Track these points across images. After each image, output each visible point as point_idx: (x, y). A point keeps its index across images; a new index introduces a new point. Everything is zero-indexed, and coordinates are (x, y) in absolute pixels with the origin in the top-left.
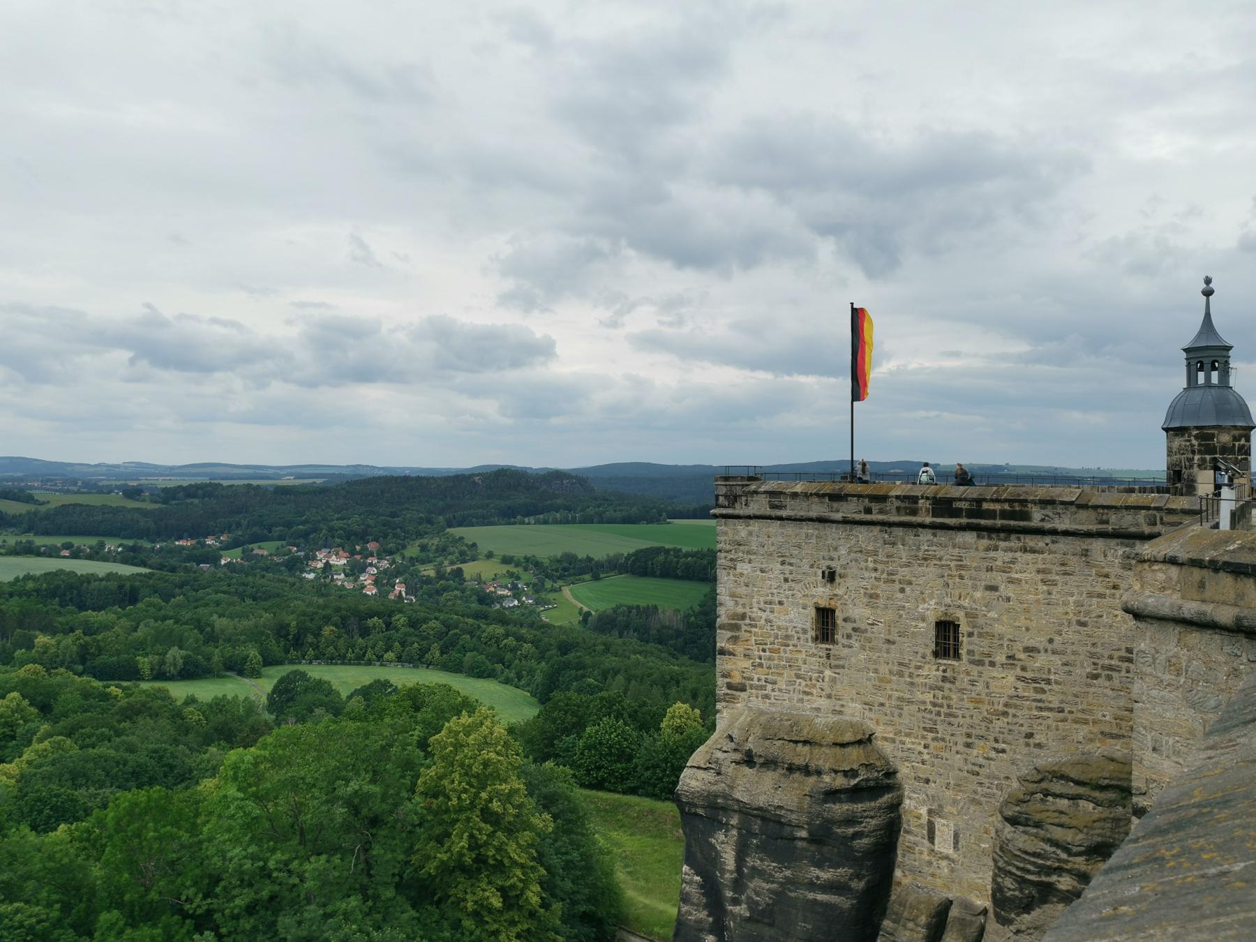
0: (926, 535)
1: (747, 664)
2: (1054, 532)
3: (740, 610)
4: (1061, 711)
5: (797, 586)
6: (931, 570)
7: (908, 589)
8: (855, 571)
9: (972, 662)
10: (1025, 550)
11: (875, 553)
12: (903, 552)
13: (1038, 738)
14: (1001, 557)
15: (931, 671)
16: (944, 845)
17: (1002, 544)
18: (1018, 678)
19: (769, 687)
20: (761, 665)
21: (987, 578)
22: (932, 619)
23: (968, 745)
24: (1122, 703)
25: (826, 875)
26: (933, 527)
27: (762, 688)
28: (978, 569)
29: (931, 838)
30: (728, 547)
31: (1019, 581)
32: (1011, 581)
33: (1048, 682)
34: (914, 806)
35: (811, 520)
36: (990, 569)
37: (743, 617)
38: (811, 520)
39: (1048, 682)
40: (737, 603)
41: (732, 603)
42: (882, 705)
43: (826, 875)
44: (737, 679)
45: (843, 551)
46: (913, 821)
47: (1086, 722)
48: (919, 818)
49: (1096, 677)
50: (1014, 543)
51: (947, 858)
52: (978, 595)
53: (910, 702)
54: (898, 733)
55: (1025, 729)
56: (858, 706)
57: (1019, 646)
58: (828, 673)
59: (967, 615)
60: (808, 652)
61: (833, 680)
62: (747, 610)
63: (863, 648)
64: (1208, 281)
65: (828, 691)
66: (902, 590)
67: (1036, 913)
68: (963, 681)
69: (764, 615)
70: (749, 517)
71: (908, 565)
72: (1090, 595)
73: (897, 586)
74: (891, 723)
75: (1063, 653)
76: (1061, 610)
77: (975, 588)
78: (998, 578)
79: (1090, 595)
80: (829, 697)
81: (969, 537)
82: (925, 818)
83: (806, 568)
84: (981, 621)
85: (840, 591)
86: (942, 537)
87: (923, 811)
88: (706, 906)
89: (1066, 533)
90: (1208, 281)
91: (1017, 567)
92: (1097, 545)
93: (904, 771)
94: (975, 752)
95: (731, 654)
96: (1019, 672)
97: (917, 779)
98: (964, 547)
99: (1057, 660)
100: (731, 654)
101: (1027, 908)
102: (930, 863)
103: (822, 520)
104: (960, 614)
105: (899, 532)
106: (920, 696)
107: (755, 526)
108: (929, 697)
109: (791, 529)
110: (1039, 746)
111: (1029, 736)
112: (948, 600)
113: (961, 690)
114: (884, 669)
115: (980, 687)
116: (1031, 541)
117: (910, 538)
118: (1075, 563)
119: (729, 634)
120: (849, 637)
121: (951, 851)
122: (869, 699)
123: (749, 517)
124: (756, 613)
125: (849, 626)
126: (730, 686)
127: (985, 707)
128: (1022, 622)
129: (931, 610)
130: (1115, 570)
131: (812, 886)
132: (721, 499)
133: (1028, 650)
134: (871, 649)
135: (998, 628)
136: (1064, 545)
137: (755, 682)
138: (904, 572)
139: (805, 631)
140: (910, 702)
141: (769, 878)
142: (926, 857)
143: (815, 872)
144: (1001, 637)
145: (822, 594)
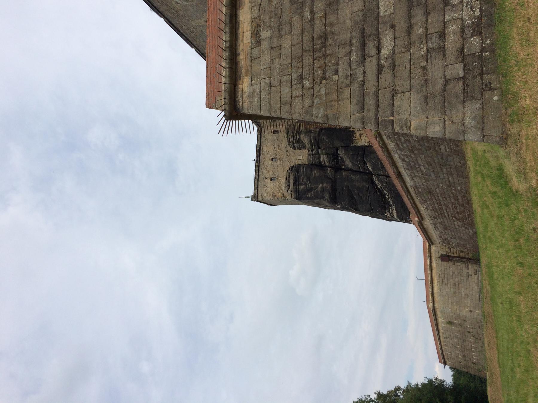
0: (261, 164)
1: (279, 193)
2: (260, 146)
3: (271, 195)
4: (282, 144)
5: (268, 184)
6: (265, 162)
7: (267, 166)
8: (265, 174)
9: (277, 156)
10: (262, 150)
11: (263, 171)
12: (263, 167)
13: (286, 146)
14: (263, 153)
15: (278, 162)
16: (301, 157)
17: (262, 153)
18: (278, 149)
19: (283, 189)
20: (279, 191)
21: (266, 154)
22: (271, 162)
23: (287, 155)
24: (280, 136)
25: (302, 169)
26: (259, 162)
27: (283, 190)
28: (265, 156)
29: (300, 159)
30: (262, 198)
31: (266, 150)
32: (266, 151)
33: (278, 145)
34: (296, 163)
35: (258, 182)
36: (265, 154)
37: (272, 194)
38: (258, 182)
39: (278, 145)
40: (270, 196)
41: (270, 197)
42: (283, 169)
43: (302, 169)
44: (282, 195)
45: (263, 177)
46: (299, 163)
47: (283, 140)
48: (298, 162)
49: (277, 140)
50: (262, 151)
51: (302, 157)
52: (268, 156)
53: (283, 165)
54: (287, 166)
55: (285, 148)
56: (284, 173)
57: (274, 150)
58: (280, 178)
59: (271, 157)
60: (277, 182)
61: (281, 178)
62: (271, 194)
63: (276, 173)
64: (253, 160)
65: (282, 178)
66: (268, 167)
67: (302, 140)
68: (279, 157)
69: (272, 190)
70: (257, 193)
71: (264, 166)
72: (268, 141)
73: (267, 168)
74: (286, 167)
75: (275, 144)
76: (270, 145)
77: (267, 156)
78: (266, 153)
79: (268, 141)
80: (283, 178)
81: (261, 157)
82: (298, 161)
83: (265, 183)
84: (271, 155)
85: (268, 177)
86: (261, 161)
87: (297, 161)
88: (312, 192)
89: (260, 144)
90: (253, 160)
91: (264, 151)
92: (262, 141)
93: (292, 165)
94: (288, 155)
95: (278, 196)
96: (277, 149)
97: (293, 162)
98: (262, 157)
99: (276, 144)
100: (278, 196)
101: (302, 141)
102: (304, 159)
103: (258, 180)
104: (271, 158)
105: (260, 168)
106: (282, 163)
107: (259, 193)
108: (282, 162)
109: (259, 186)
110: (286, 146)
111: (285, 147)
112: (269, 160)
113: (280, 157)
114: (279, 169)
115: (280, 154)
116: (261, 149)
117: (261, 166)
118: (264, 143)
119: (275, 197)
120: (274, 175)
121: (301, 157)
122: (283, 171)
123: (257, 193)
124: (271, 192)
125: (273, 175)
126: (283, 197)
127: (282, 154)
128: (271, 149)
129: (270, 162)
130: (265, 139)
131: (303, 171)
132: (255, 199)
133: (275, 148)
134: (276, 171)
135: (272, 152)
136: (262, 145)
137: (282, 192)
138: (265, 167)
139: (274, 183)
140: (283, 165)
141: (303, 178)
142: (303, 160)
143: (302, 171)
144: (273, 152)
145: (268, 180)
